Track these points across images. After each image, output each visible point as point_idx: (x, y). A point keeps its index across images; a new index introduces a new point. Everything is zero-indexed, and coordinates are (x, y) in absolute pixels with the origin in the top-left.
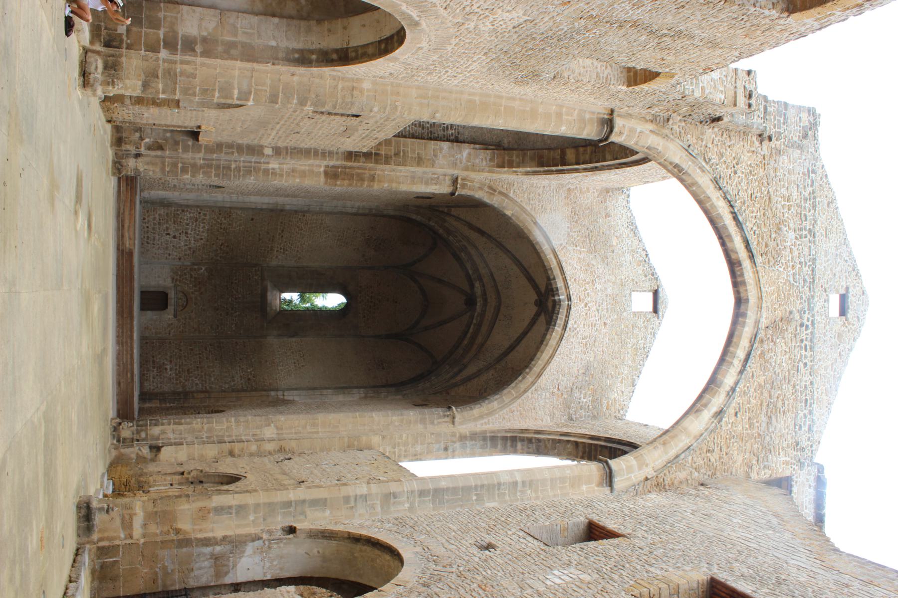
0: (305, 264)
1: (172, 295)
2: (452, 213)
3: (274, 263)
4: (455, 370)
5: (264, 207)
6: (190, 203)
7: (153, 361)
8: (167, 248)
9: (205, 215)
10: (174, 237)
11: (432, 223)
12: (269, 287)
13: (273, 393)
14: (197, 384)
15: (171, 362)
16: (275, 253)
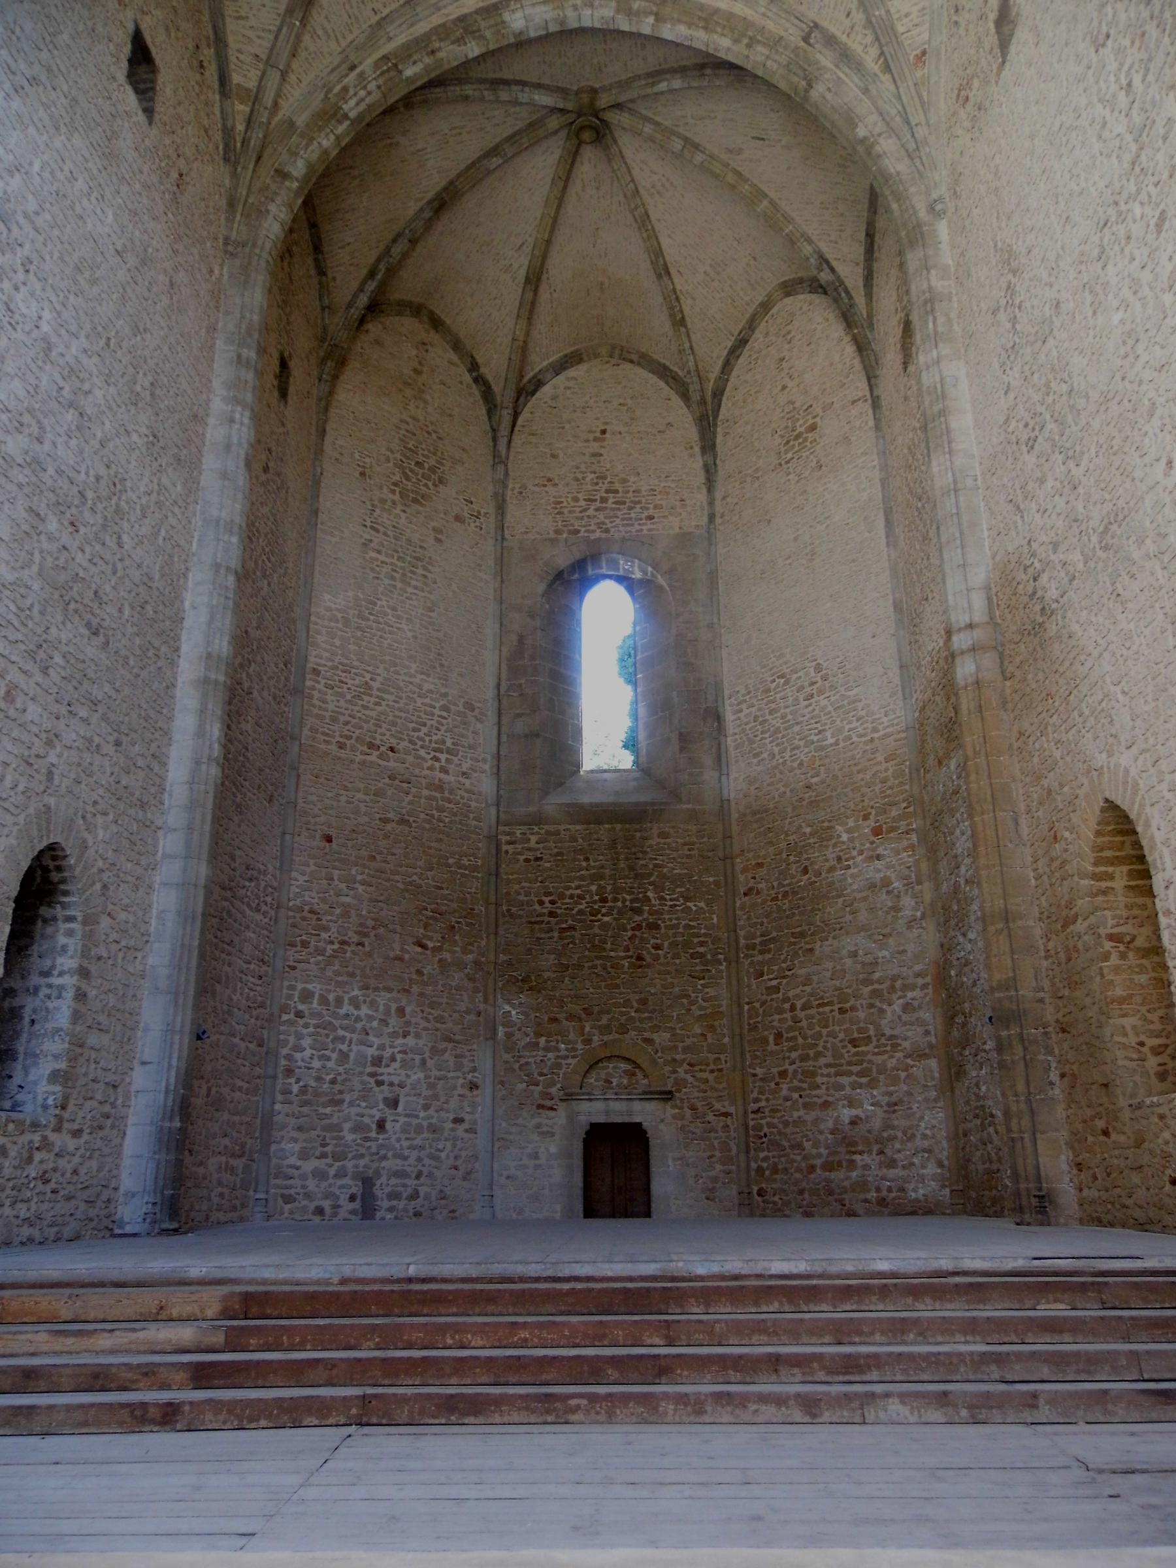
0: (490, 694)
1: (595, 1111)
2: (252, 84)
3: (486, 785)
4: (826, 59)
5: (216, 731)
6: (184, 1019)
7: (829, 1167)
8: (434, 1129)
9: (306, 996)
10: (394, 1103)
11: (298, 169)
12: (565, 799)
13: (965, 669)
14: (907, 1007)
15: (826, 1105)
16: (451, 778)
